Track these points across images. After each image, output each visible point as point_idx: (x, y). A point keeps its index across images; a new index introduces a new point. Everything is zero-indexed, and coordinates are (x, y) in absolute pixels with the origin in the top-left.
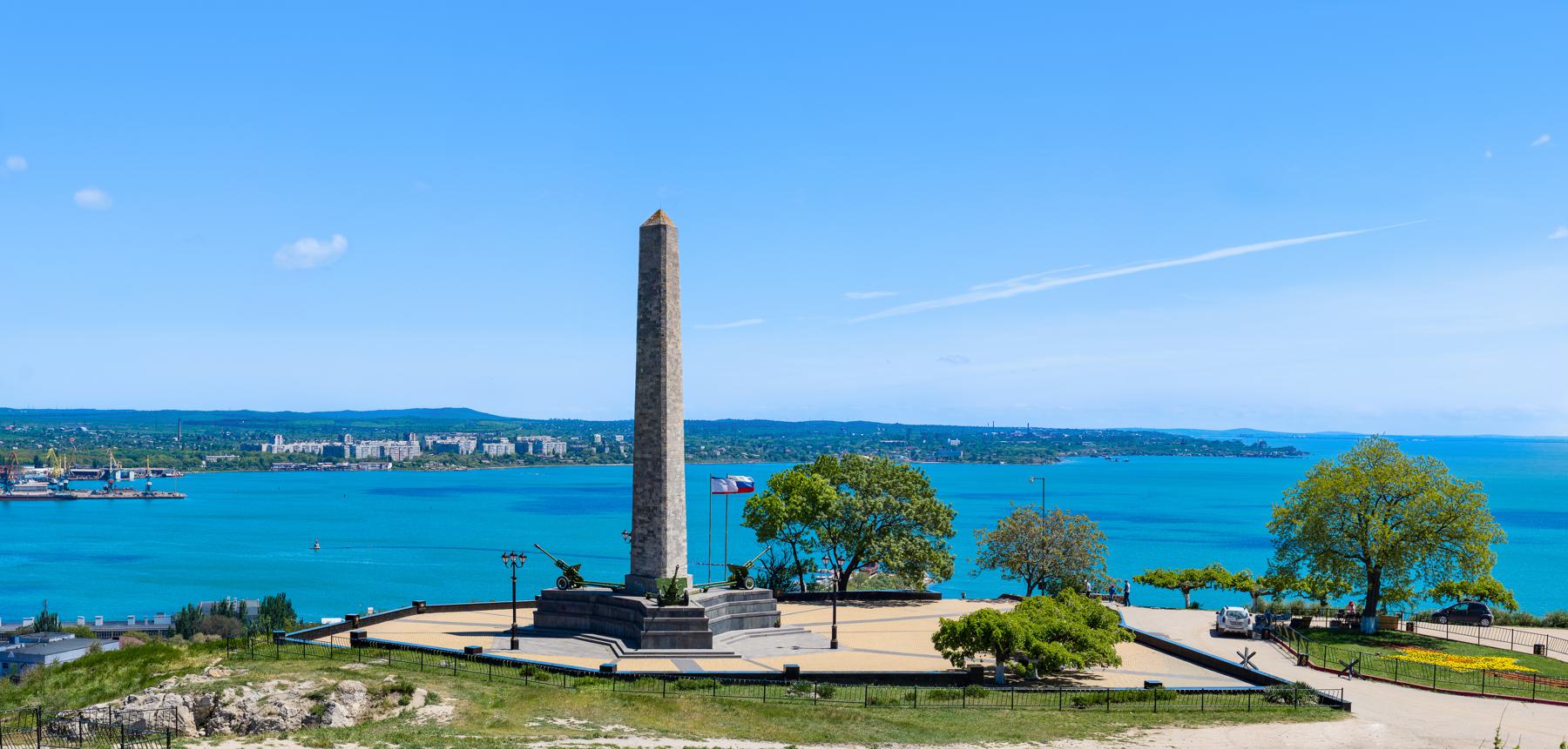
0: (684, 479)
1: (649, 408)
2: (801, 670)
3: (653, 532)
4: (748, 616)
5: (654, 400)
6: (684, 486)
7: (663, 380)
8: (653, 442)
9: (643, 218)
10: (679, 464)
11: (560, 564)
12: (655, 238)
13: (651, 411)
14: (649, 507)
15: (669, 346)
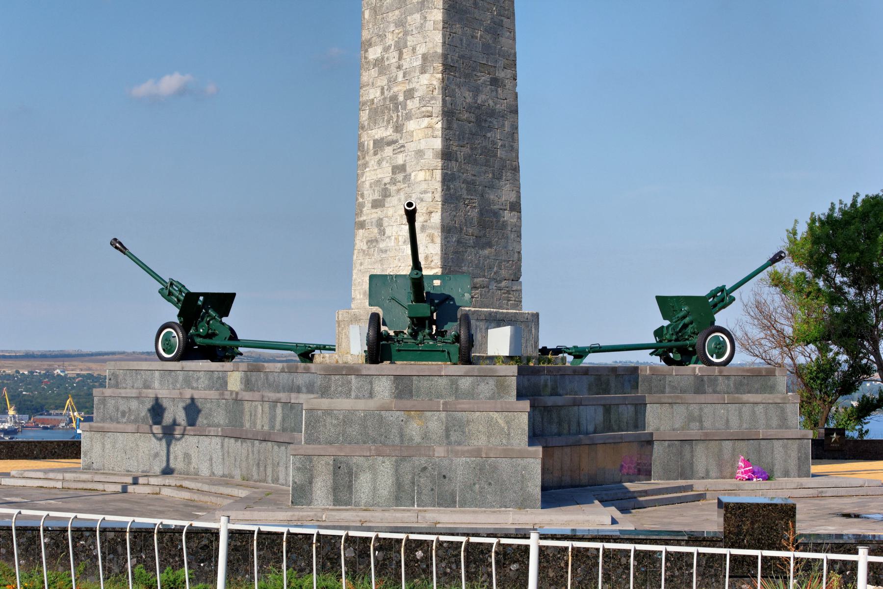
11: (169, 291)
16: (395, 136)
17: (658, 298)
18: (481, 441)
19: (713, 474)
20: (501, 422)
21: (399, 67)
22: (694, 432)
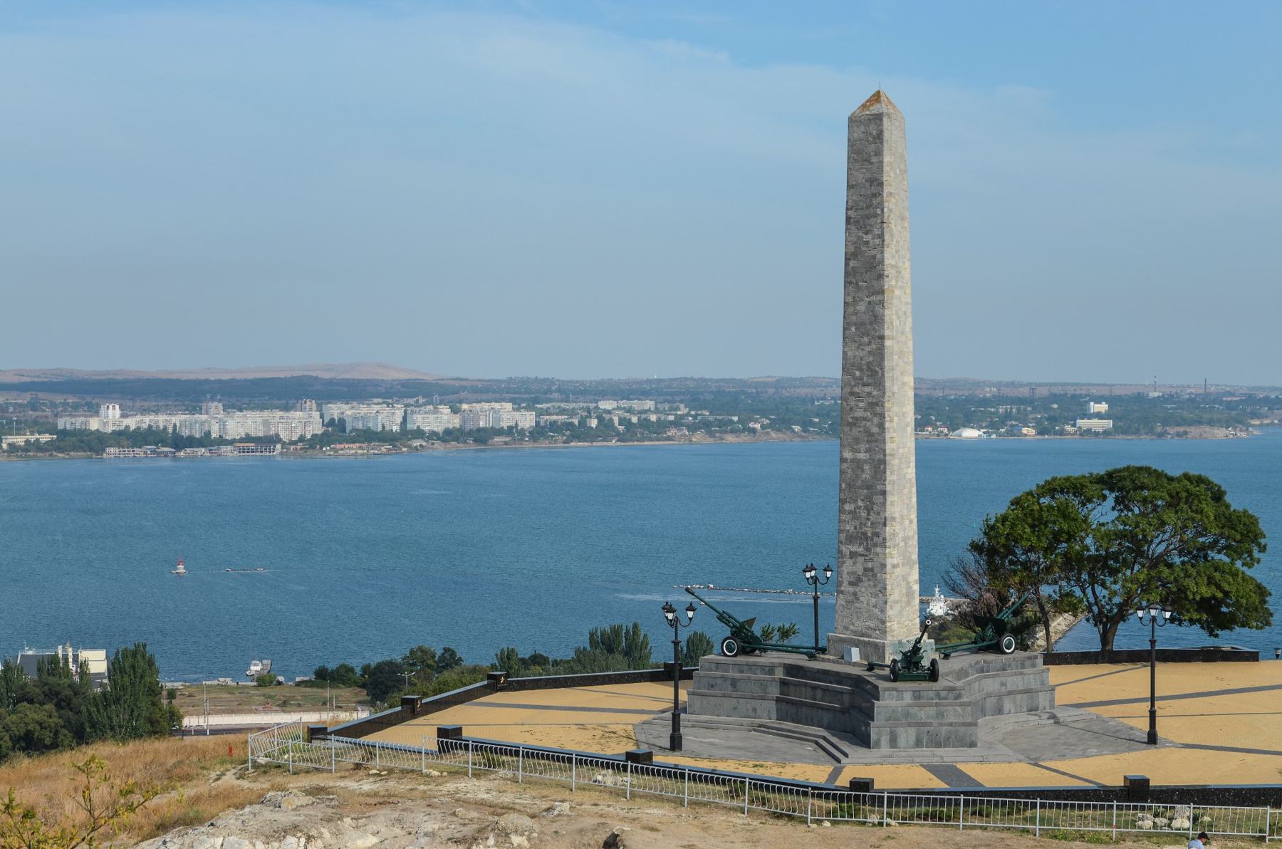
0: (914, 490)
1: (868, 385)
2: (1151, 784)
4: (1010, 693)
5: (873, 374)
7: (888, 343)
8: (872, 435)
9: (853, 102)
10: (909, 467)
12: (875, 132)
13: (867, 389)
14: (865, 534)
15: (897, 292)
16: (865, 553)
18: (952, 720)
19: (1012, 711)
20: (960, 711)
21: (868, 519)
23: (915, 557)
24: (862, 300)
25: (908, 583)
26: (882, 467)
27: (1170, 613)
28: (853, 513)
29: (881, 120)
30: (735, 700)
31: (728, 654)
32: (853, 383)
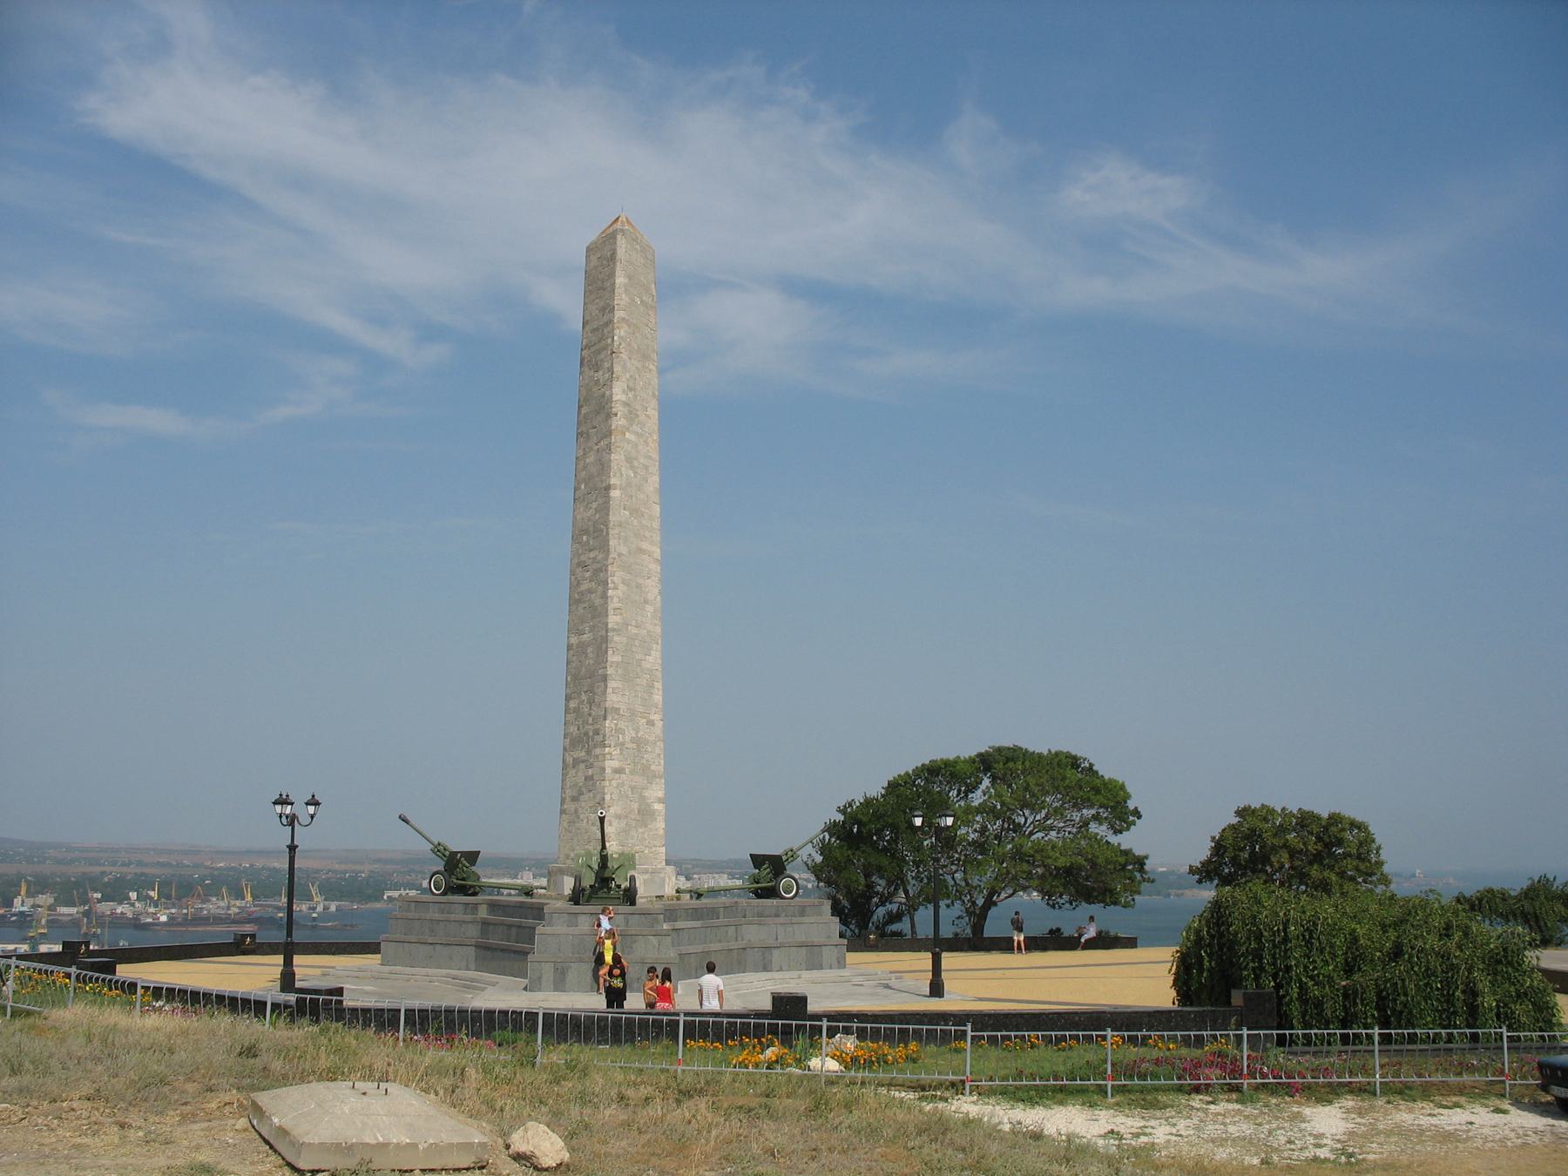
3: (592, 778)
6: (658, 697)
13: (592, 555)
17: (751, 855)
21: (590, 715)
22: (771, 942)
23: (658, 766)
24: (591, 449)
25: (642, 798)
26: (604, 646)
27: (952, 819)
28: (577, 710)
29: (615, 238)
30: (431, 947)
31: (434, 891)
32: (580, 551)
